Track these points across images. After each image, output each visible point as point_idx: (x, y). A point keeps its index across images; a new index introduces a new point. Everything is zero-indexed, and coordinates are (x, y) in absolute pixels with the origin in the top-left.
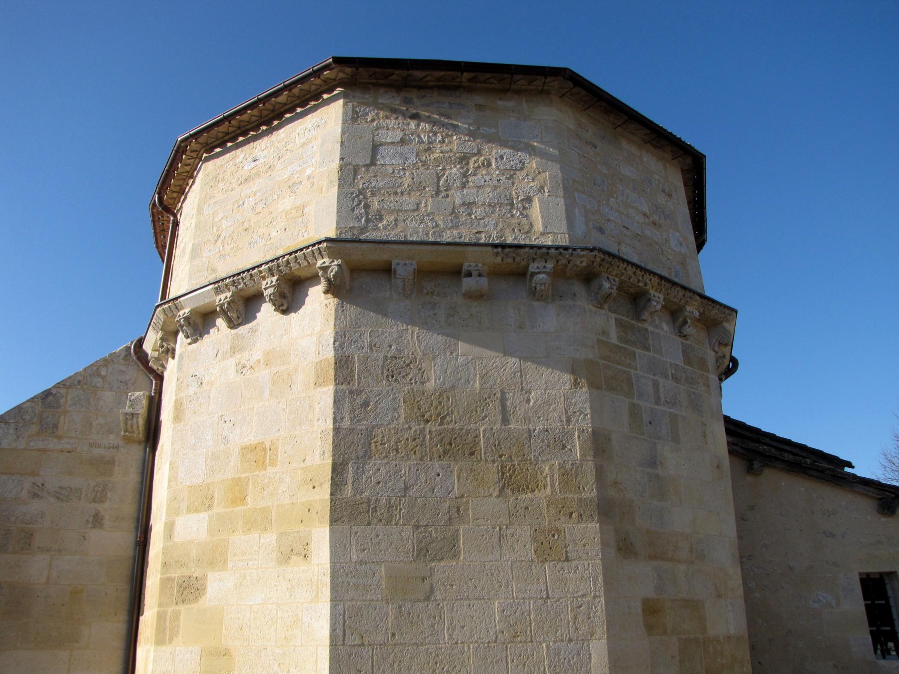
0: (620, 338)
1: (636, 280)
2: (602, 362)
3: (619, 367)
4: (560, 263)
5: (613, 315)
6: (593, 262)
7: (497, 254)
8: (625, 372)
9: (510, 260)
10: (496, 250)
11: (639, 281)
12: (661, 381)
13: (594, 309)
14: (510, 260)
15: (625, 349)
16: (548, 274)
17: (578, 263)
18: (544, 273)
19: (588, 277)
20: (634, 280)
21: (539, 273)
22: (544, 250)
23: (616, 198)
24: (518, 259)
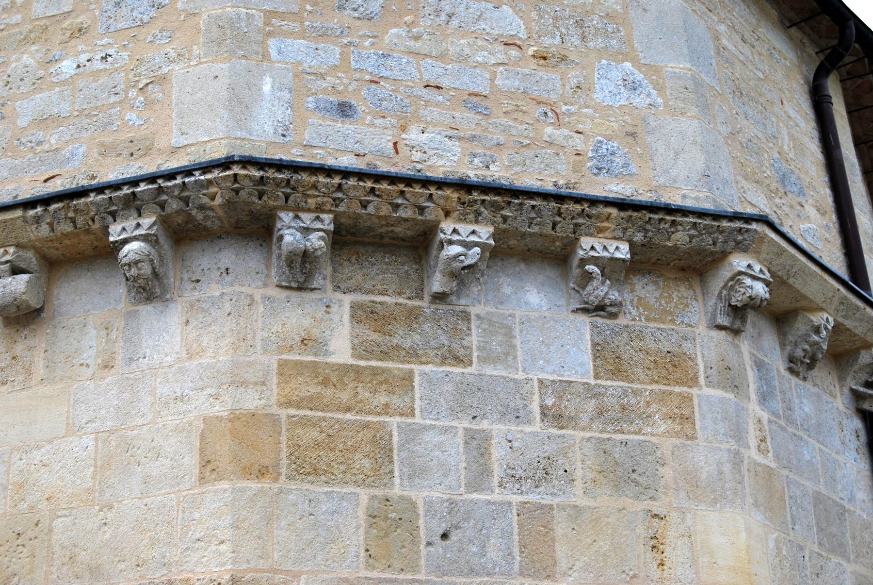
0: (362, 349)
1: (385, 210)
2: (284, 413)
3: (349, 416)
4: (168, 210)
5: (348, 299)
6: (237, 191)
7: (38, 220)
8: (367, 425)
9: (68, 228)
10: (31, 212)
11: (396, 207)
12: (497, 429)
13: (285, 294)
14: (68, 228)
15: (375, 372)
16: (145, 238)
17: (205, 200)
18: (135, 238)
19: (254, 229)
20: (378, 208)
21: (126, 241)
22: (126, 190)
23: (410, 26)
24: (80, 221)
